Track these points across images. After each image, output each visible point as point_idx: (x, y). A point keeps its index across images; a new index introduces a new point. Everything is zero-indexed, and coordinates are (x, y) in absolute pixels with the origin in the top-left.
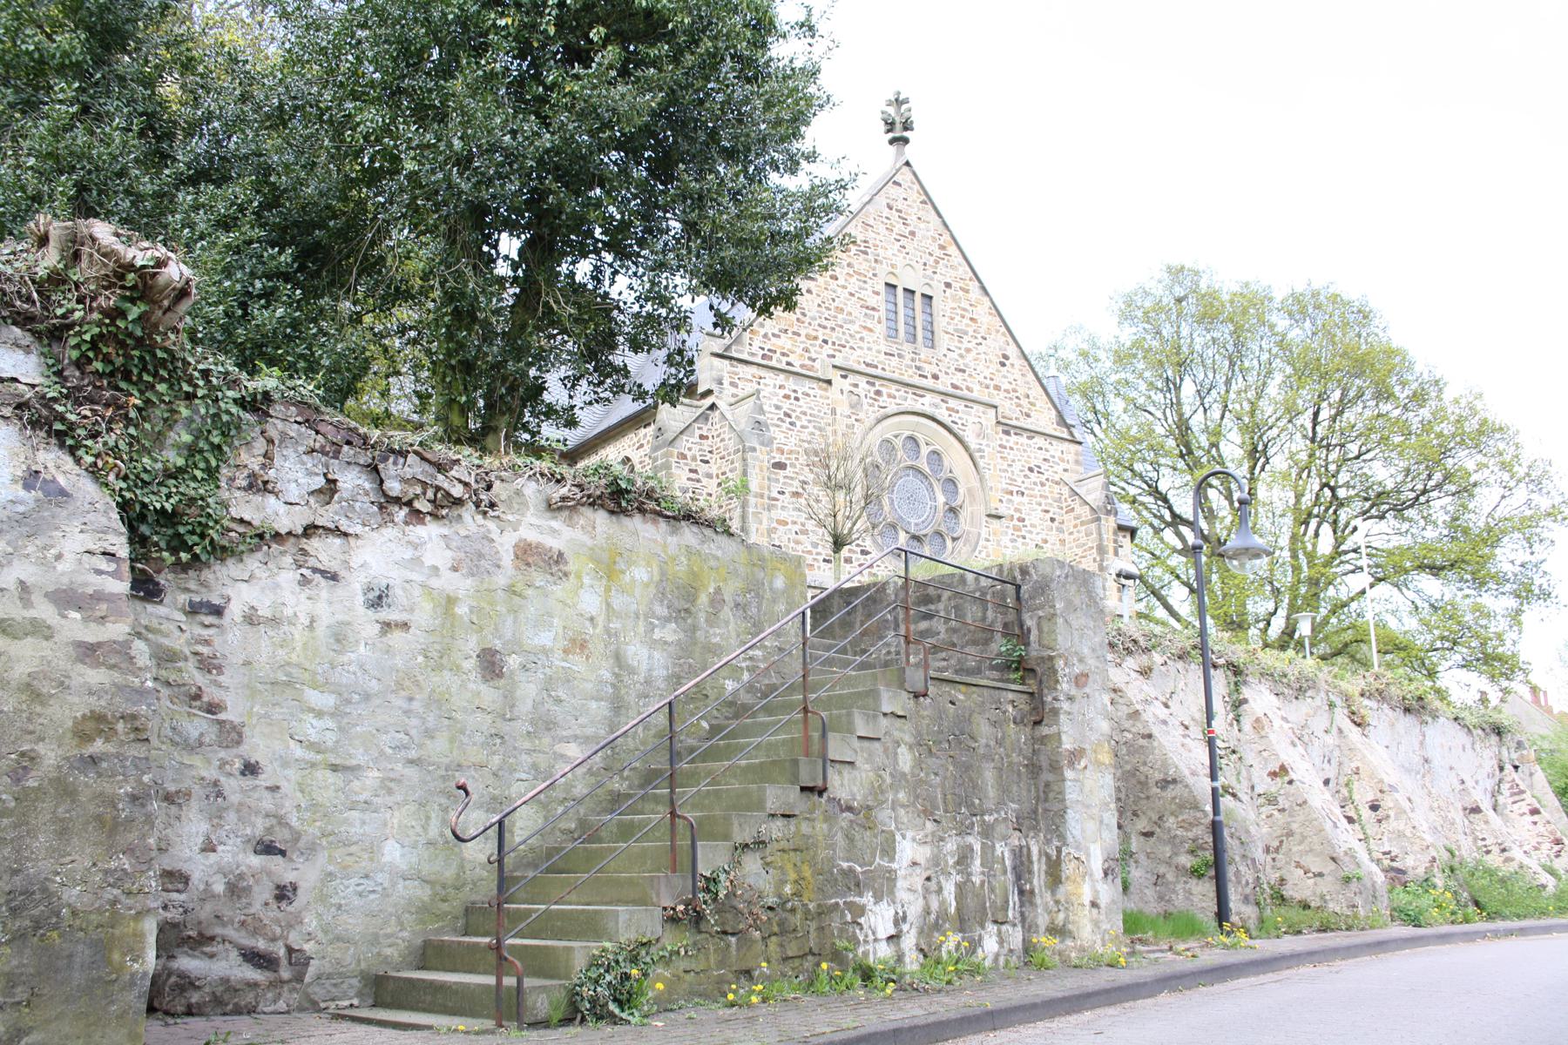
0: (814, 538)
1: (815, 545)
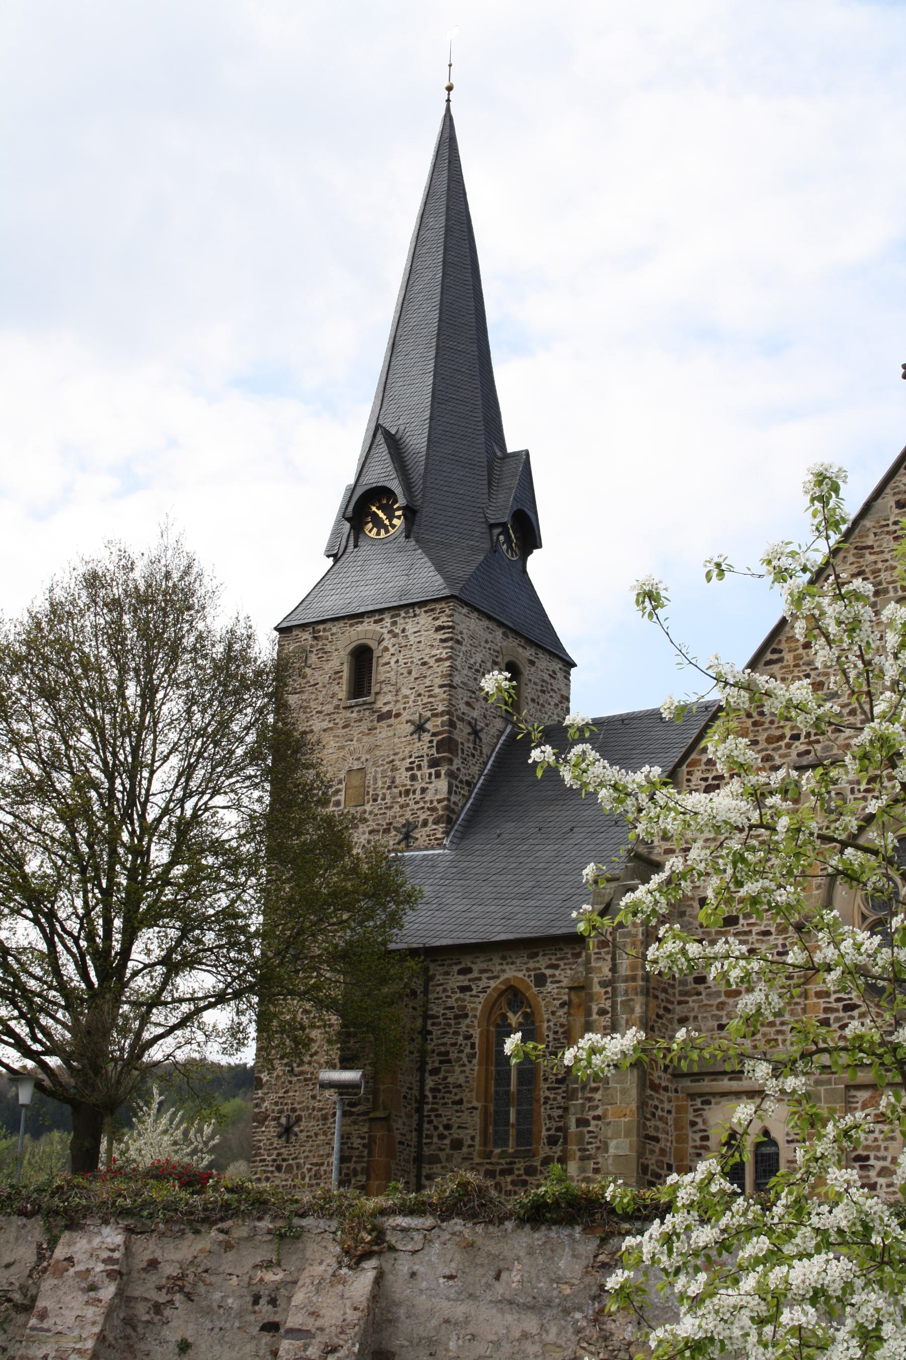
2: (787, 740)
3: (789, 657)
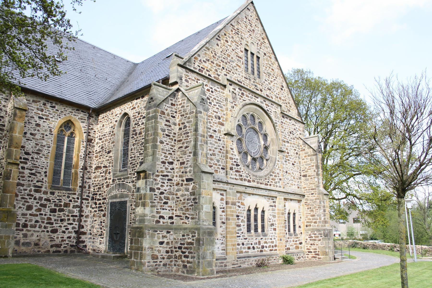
0: (218, 158)
1: (218, 161)
3: (222, 41)
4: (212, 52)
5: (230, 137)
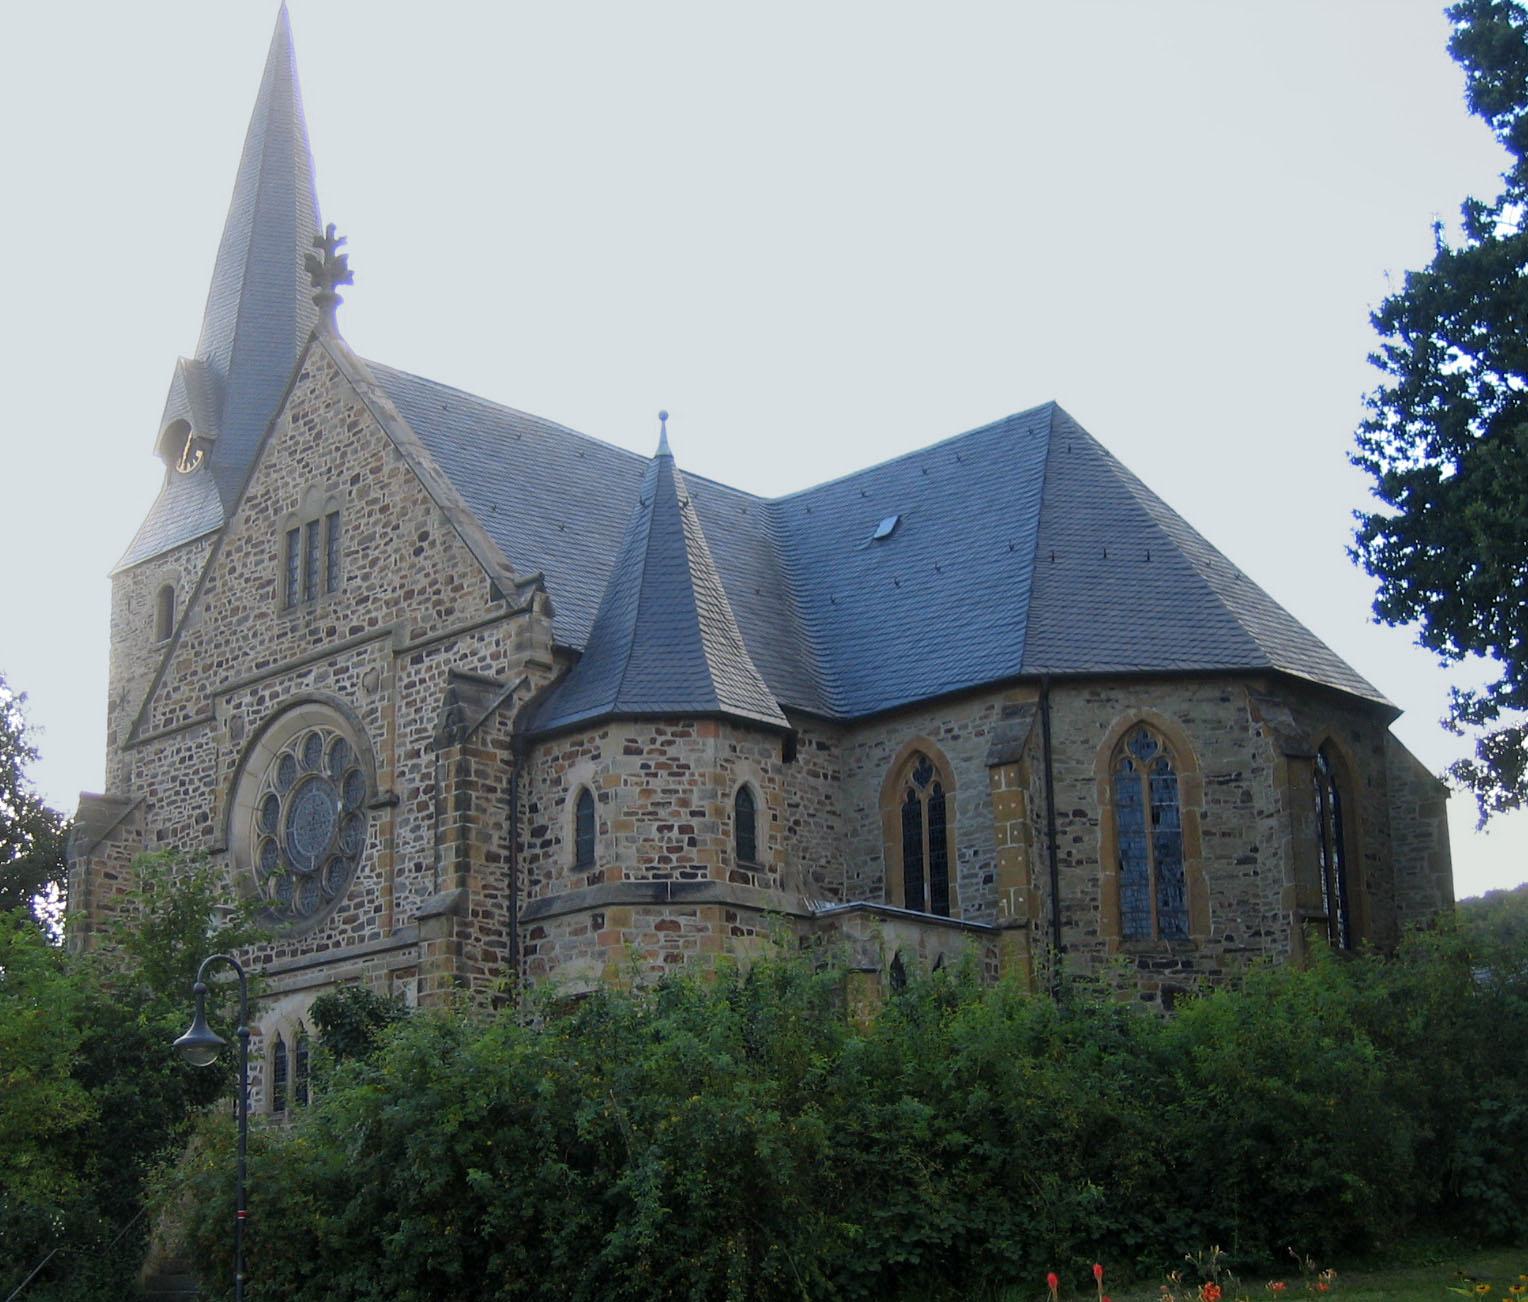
2: (215, 668)
4: (193, 647)
5: (219, 857)
